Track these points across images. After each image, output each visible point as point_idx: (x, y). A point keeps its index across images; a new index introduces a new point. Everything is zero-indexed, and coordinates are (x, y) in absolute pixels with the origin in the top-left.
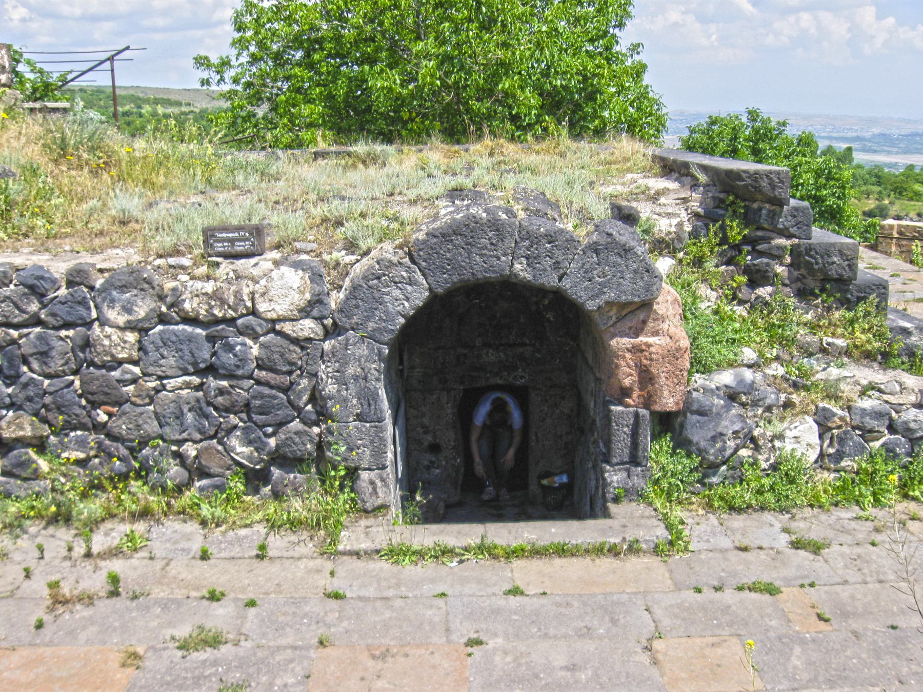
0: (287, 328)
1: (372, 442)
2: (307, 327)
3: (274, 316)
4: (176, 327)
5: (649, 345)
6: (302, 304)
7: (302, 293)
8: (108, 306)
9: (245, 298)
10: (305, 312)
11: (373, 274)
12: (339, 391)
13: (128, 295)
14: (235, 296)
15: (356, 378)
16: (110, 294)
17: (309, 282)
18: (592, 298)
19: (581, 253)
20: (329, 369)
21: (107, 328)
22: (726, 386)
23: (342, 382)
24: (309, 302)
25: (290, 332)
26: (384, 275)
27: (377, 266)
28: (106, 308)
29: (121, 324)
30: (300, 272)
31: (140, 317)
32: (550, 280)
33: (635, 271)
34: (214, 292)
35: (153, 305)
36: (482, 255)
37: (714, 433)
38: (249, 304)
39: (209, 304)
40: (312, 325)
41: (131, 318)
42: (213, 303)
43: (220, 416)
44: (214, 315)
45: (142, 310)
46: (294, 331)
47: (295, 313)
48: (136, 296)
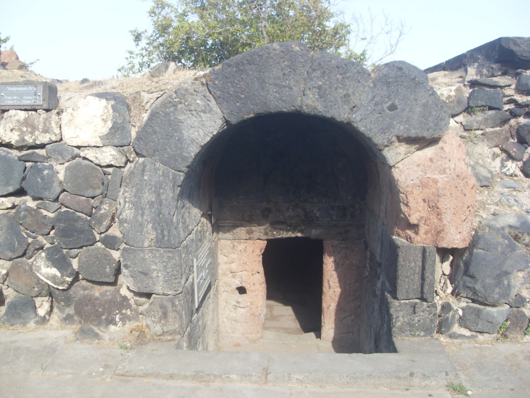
0: (90, 154)
1: (165, 267)
2: (108, 155)
5: (435, 182)
9: (53, 124)
11: (170, 102)
12: (135, 217)
14: (45, 123)
15: (151, 204)
17: (111, 111)
18: (383, 131)
19: (372, 85)
20: (126, 194)
22: (511, 227)
23: (137, 205)
25: (92, 159)
26: (181, 103)
27: (175, 95)
30: (104, 102)
32: (341, 114)
33: (425, 105)
34: (26, 119)
36: (276, 85)
37: (499, 272)
38: (57, 131)
39: (20, 129)
40: (114, 152)
43: (29, 236)
44: (24, 140)
46: (97, 158)
47: (99, 140)
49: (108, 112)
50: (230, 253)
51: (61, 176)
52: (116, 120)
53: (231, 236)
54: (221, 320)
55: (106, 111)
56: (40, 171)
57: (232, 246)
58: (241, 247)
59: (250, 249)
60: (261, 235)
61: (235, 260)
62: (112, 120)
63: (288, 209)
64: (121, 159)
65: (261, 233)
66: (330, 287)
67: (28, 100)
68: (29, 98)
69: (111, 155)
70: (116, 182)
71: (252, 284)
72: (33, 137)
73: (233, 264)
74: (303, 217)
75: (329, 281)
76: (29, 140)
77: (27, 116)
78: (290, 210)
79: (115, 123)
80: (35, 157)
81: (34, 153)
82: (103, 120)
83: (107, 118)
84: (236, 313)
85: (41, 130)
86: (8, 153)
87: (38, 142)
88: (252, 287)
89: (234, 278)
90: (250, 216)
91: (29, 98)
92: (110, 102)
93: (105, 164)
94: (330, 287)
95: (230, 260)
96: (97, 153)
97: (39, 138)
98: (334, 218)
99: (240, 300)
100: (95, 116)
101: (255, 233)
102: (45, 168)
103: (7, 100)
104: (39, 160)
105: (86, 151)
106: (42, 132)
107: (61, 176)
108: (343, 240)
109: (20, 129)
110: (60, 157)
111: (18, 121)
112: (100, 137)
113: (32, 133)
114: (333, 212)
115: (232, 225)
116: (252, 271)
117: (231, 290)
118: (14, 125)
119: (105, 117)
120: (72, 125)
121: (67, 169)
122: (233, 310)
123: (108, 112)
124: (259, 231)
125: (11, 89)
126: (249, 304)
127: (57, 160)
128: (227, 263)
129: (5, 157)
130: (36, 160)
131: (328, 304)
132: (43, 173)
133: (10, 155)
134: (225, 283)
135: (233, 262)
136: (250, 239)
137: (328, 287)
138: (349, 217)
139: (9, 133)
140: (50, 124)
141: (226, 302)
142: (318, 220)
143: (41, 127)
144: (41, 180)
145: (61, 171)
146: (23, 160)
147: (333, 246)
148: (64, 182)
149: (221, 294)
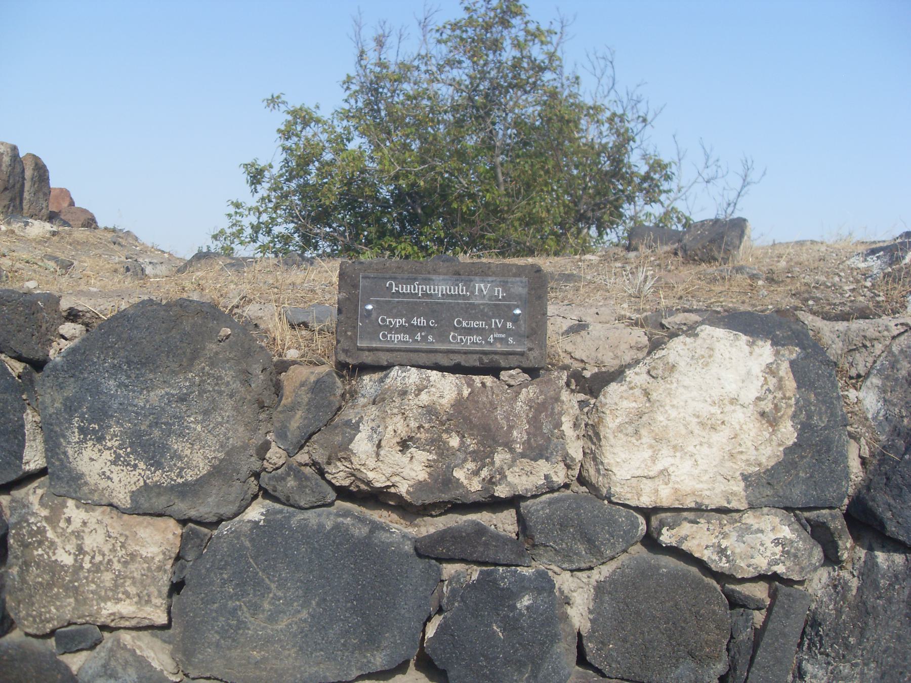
0: (699, 539)
2: (765, 543)
3: (665, 496)
4: (312, 517)
6: (768, 454)
7: (770, 419)
8: (82, 430)
10: (769, 488)
13: (155, 396)
14: (535, 422)
16: (95, 389)
17: (791, 384)
21: (71, 509)
24: (789, 451)
25: (707, 555)
28: (76, 437)
29: (123, 498)
30: (765, 351)
31: (190, 476)
34: (459, 403)
35: (238, 435)
38: (575, 450)
40: (786, 532)
41: (158, 476)
42: (454, 442)
44: (448, 481)
45: (196, 458)
46: (722, 552)
47: (738, 487)
48: (182, 399)
49: (780, 387)
51: (579, 614)
52: (809, 416)
55: (772, 381)
56: (511, 595)
62: (794, 417)
64: (810, 555)
67: (469, 331)
68: (474, 324)
69: (777, 542)
70: (784, 635)
72: (485, 473)
76: (468, 480)
77: (466, 392)
79: (805, 428)
80: (486, 545)
81: (480, 530)
82: (763, 414)
83: (777, 408)
85: (519, 448)
86: (376, 527)
87: (501, 491)
91: (474, 324)
92: (784, 351)
93: (750, 573)
96: (725, 536)
97: (510, 478)
100: (734, 401)
102: (523, 586)
103: (386, 327)
104: (501, 557)
105: (686, 528)
106: (523, 455)
107: (579, 614)
109: (436, 444)
110: (581, 548)
111: (430, 411)
112: (745, 477)
113: (482, 457)
118: (414, 424)
119: (767, 406)
120: (644, 432)
121: (600, 589)
123: (780, 387)
125: (406, 289)
127: (566, 557)
129: (366, 544)
130: (491, 555)
132: (514, 607)
133: (383, 536)
139: (392, 455)
140: (558, 425)
143: (519, 435)
144: (504, 630)
145: (579, 596)
146: (431, 552)
148: (591, 637)
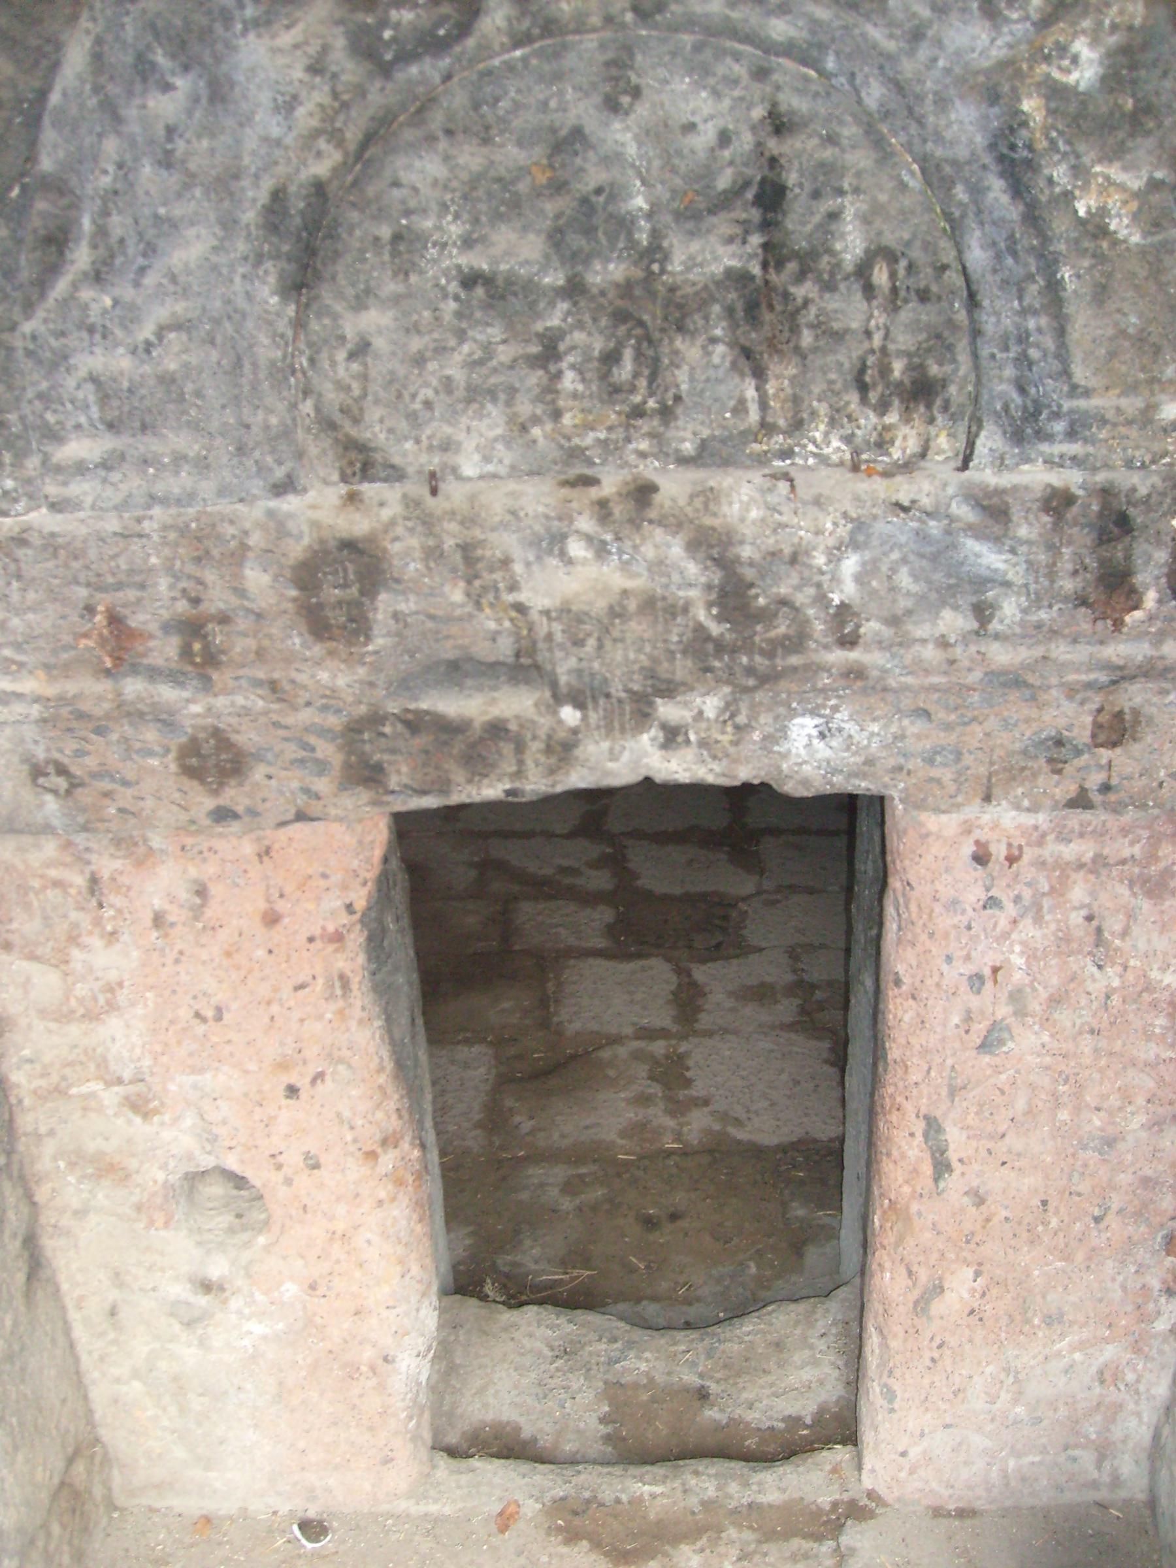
50: (73, 939)
53: (51, 804)
54: (99, 1394)
57: (79, 880)
58: (163, 885)
59: (237, 907)
60: (322, 785)
61: (122, 997)
63: (553, 543)
65: (321, 767)
66: (942, 1167)
71: (293, 1159)
73: (114, 1025)
74: (701, 614)
75: (933, 1126)
78: (576, 549)
84: (202, 1343)
88: (304, 1181)
89: (146, 1115)
90: (192, 629)
94: (942, 1167)
95: (81, 990)
98: (1010, 609)
99: (217, 1269)
101: (258, 773)
108: (1081, 801)
114: (990, 558)
115: (35, 710)
116: (283, 1066)
117: (139, 1208)
122: (177, 1327)
124: (292, 751)
126: (291, 1290)
128: (63, 1016)
131: (923, 1275)
134: (77, 1159)
135: (112, 1007)
136: (223, 815)
137: (927, 1169)
138: (1150, 598)
141: (118, 1278)
142: (849, 641)
147: (981, 858)
149: (68, 1233)
